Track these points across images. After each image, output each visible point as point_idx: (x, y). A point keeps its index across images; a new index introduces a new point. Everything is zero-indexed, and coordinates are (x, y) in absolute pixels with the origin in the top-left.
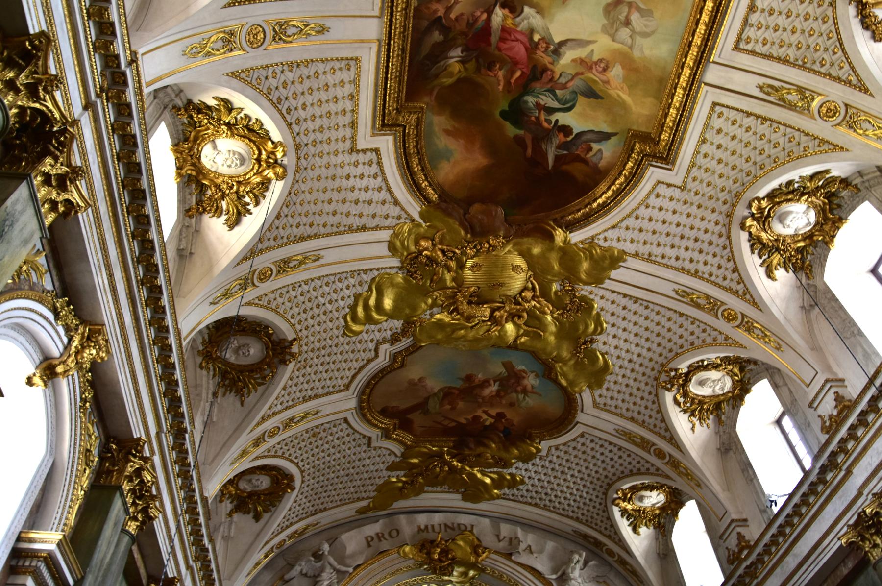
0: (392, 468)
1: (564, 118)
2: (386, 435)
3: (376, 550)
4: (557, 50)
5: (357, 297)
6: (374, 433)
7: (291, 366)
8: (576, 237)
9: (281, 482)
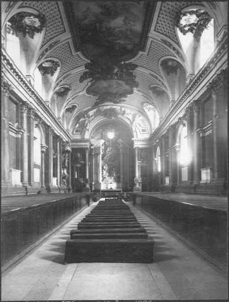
0: (97, 100)
1: (119, 41)
2: (94, 95)
3: (96, 115)
4: (114, 29)
5: (81, 77)
6: (92, 96)
7: (70, 92)
8: (127, 62)
9: (74, 107)
